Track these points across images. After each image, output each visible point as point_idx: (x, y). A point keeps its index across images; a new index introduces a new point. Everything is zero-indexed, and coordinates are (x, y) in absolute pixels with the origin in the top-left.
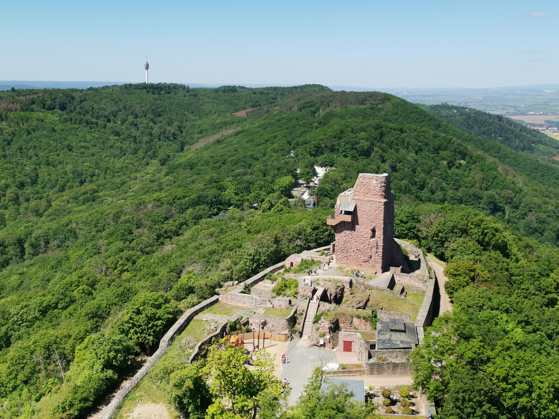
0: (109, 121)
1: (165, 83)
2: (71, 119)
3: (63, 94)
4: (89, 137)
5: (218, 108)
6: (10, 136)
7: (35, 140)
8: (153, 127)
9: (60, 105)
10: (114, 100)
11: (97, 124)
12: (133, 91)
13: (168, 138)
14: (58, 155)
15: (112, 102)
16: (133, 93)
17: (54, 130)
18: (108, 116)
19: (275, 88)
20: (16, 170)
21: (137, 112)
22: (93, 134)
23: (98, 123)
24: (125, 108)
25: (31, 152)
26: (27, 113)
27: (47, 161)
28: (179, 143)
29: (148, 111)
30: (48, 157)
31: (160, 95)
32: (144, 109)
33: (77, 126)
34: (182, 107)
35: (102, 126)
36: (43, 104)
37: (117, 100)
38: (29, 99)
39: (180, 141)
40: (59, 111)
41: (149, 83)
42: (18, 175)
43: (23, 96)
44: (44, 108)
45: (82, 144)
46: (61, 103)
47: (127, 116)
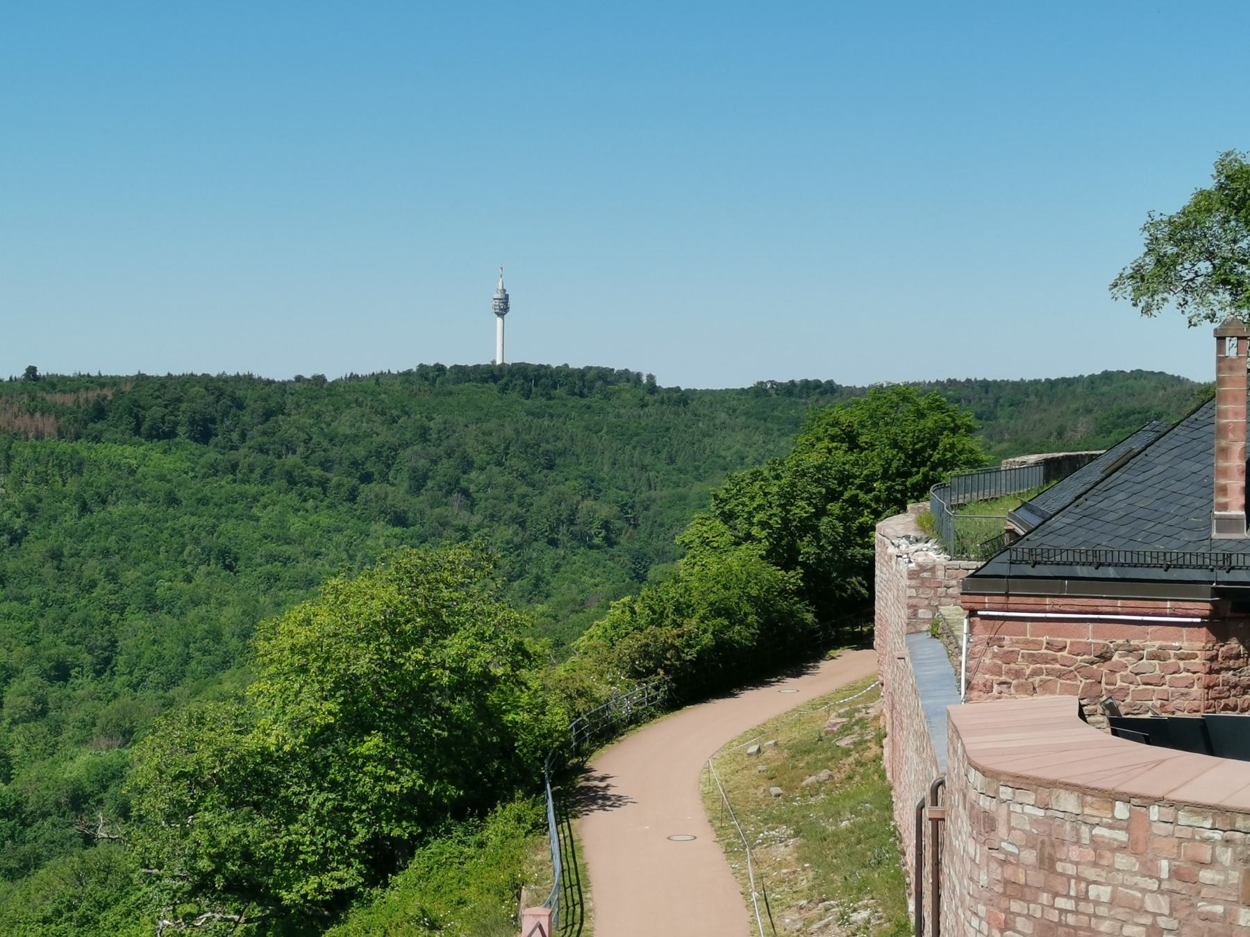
0: (367, 478)
1: (566, 365)
2: (234, 467)
3: (206, 389)
4: (296, 524)
5: (771, 447)
6: (19, 517)
7: (104, 529)
8: (528, 500)
9: (192, 422)
10: (383, 414)
11: (323, 484)
12: (450, 387)
13: (583, 540)
14: (188, 579)
15: (378, 419)
16: (450, 393)
17: (173, 500)
18: (363, 464)
19: (986, 386)
20: (42, 623)
21: (470, 450)
22: (313, 518)
23: (328, 480)
24: (424, 435)
25: (93, 568)
26: (81, 447)
27: (149, 597)
28: (626, 558)
29: (507, 448)
30: (151, 585)
31: (550, 399)
32: (494, 440)
33: (252, 489)
34: (633, 443)
35: (344, 492)
36: (137, 417)
37: (395, 413)
38: (87, 400)
39: (628, 551)
40: (193, 446)
41: (509, 361)
42: (48, 638)
43: (64, 392)
44: (137, 431)
45: (272, 547)
46: (198, 417)
47: (434, 462)
